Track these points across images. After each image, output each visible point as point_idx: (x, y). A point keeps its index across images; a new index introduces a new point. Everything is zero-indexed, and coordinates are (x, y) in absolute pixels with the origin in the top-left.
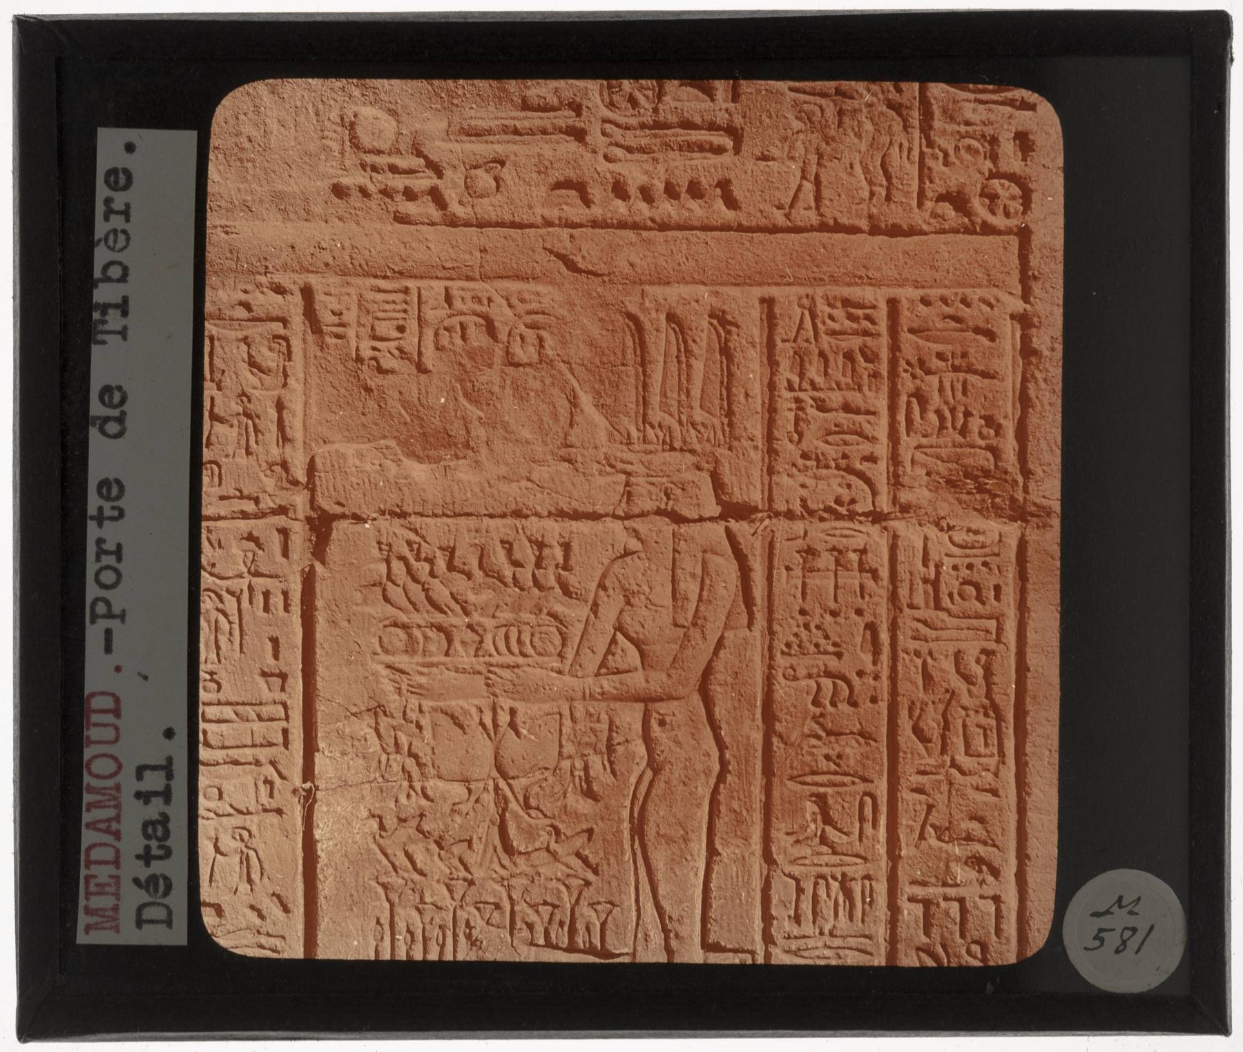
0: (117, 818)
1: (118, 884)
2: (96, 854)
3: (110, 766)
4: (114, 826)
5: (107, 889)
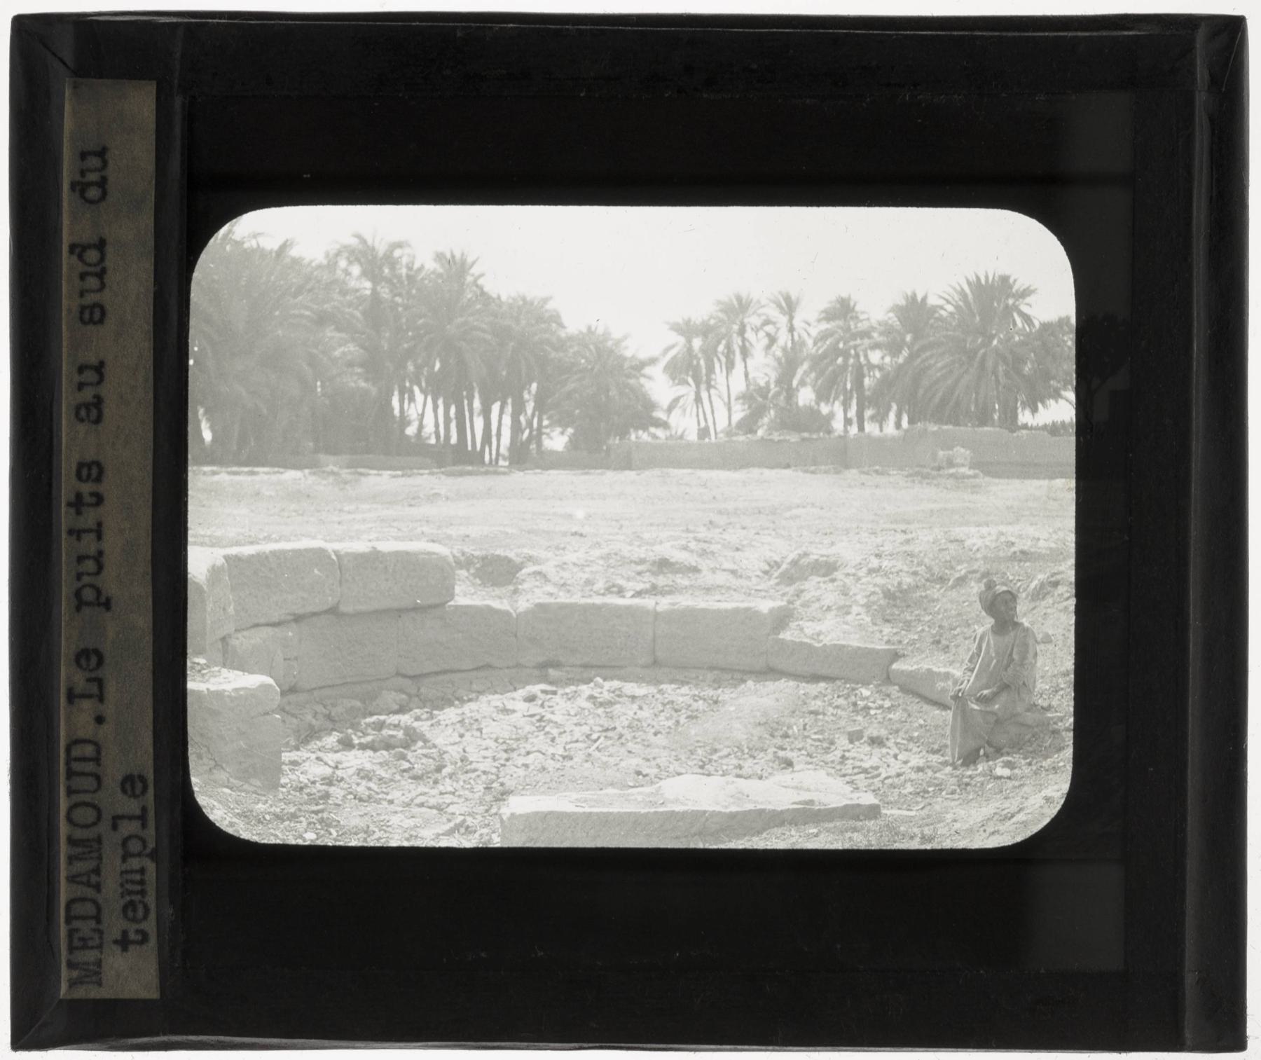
0: (97, 871)
1: (101, 938)
2: (79, 909)
3: (90, 815)
4: (94, 879)
5: (90, 943)
